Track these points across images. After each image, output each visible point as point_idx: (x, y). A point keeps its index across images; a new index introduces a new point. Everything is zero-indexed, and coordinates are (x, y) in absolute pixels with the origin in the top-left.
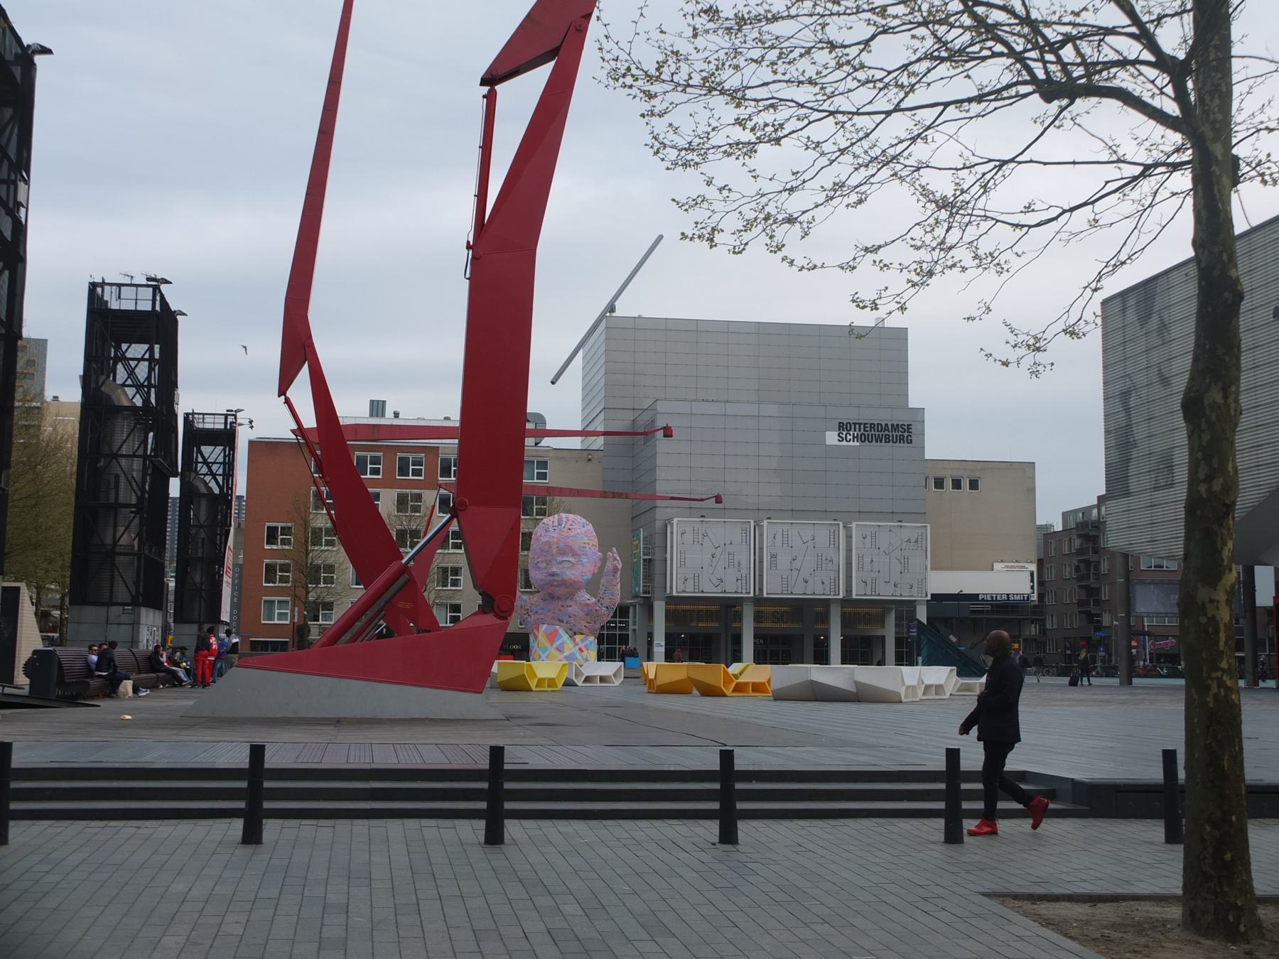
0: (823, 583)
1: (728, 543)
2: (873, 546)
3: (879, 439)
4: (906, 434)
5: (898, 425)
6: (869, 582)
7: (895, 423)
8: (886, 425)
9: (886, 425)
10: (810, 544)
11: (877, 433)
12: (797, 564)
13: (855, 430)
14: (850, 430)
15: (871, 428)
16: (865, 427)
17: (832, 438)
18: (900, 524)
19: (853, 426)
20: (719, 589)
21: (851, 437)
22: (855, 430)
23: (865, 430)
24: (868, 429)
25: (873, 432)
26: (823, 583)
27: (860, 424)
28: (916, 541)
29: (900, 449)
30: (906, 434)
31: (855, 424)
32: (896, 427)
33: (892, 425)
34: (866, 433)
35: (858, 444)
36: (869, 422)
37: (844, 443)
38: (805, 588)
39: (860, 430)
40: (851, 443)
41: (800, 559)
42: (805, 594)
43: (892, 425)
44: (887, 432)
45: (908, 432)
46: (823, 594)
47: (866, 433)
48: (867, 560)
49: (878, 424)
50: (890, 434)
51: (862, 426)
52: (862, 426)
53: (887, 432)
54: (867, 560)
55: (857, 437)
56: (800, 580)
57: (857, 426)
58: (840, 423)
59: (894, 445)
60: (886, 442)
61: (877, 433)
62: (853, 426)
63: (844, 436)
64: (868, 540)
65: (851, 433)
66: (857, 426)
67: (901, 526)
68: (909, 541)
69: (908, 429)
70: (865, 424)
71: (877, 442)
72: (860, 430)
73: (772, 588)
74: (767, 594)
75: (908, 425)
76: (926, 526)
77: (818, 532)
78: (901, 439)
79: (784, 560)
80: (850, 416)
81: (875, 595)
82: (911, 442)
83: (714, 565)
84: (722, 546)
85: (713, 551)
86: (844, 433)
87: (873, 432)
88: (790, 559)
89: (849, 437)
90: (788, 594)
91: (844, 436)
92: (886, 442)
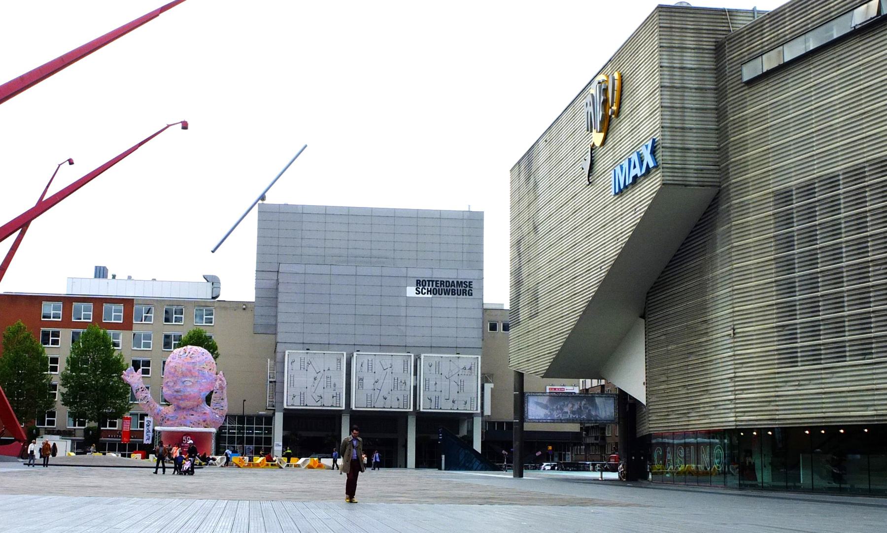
0: (398, 400)
1: (326, 369)
2: (437, 372)
3: (447, 293)
4: (468, 289)
5: (461, 282)
6: (433, 400)
7: (460, 281)
8: (453, 282)
9: (453, 282)
10: (389, 370)
11: (445, 288)
12: (378, 386)
13: (429, 286)
14: (425, 286)
15: (441, 284)
16: (436, 284)
17: (411, 291)
18: (458, 356)
19: (427, 282)
20: (319, 404)
21: (426, 291)
22: (429, 286)
23: (436, 286)
24: (439, 285)
25: (442, 287)
26: (398, 400)
27: (433, 281)
28: (470, 369)
29: (463, 300)
30: (468, 289)
31: (429, 281)
32: (460, 284)
33: (457, 282)
34: (437, 288)
35: (431, 296)
36: (440, 280)
37: (421, 295)
38: (385, 403)
39: (432, 286)
40: (426, 295)
41: (381, 381)
42: (384, 408)
43: (457, 282)
44: (453, 287)
45: (469, 287)
46: (398, 408)
47: (437, 288)
48: (432, 383)
49: (446, 281)
50: (456, 289)
51: (434, 283)
52: (434, 283)
53: (453, 287)
54: (432, 383)
55: (430, 291)
56: (381, 398)
57: (431, 283)
58: (417, 281)
59: (459, 297)
60: (452, 295)
61: (445, 288)
62: (427, 282)
63: (420, 290)
64: (433, 367)
65: (426, 288)
66: (431, 283)
67: (458, 358)
68: (465, 368)
69: (470, 285)
70: (436, 281)
71: (445, 294)
72: (432, 286)
73: (424, 407)
74: (423, 409)
75: (470, 282)
76: (478, 358)
77: (398, 361)
78: (464, 292)
79: (368, 383)
80: (425, 274)
81: (438, 409)
82: (472, 295)
83: (316, 386)
84: (322, 371)
85: (316, 375)
86: (421, 288)
87: (442, 287)
88: (373, 381)
89: (424, 291)
90: (371, 408)
91: (420, 290)
92: (452, 295)
